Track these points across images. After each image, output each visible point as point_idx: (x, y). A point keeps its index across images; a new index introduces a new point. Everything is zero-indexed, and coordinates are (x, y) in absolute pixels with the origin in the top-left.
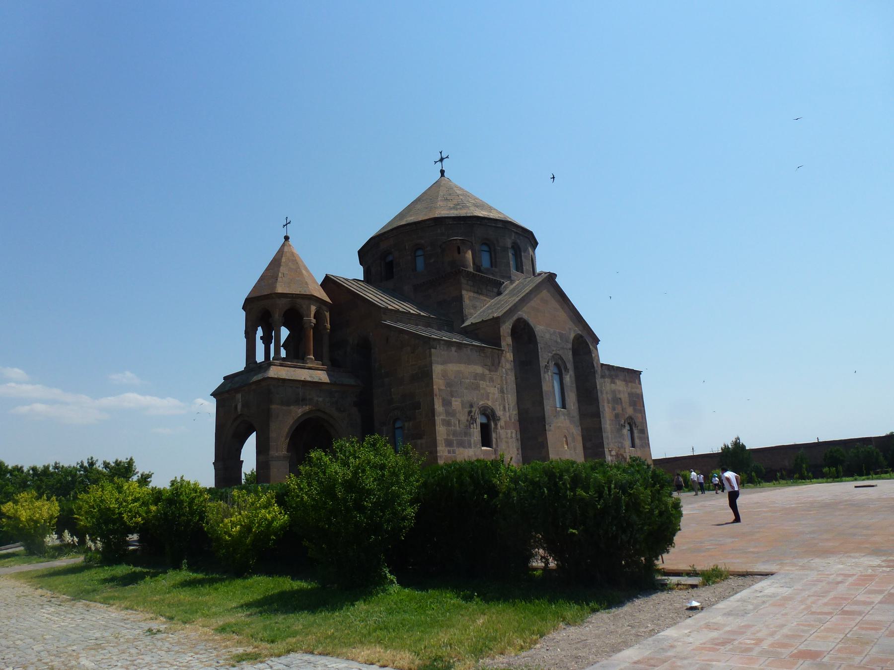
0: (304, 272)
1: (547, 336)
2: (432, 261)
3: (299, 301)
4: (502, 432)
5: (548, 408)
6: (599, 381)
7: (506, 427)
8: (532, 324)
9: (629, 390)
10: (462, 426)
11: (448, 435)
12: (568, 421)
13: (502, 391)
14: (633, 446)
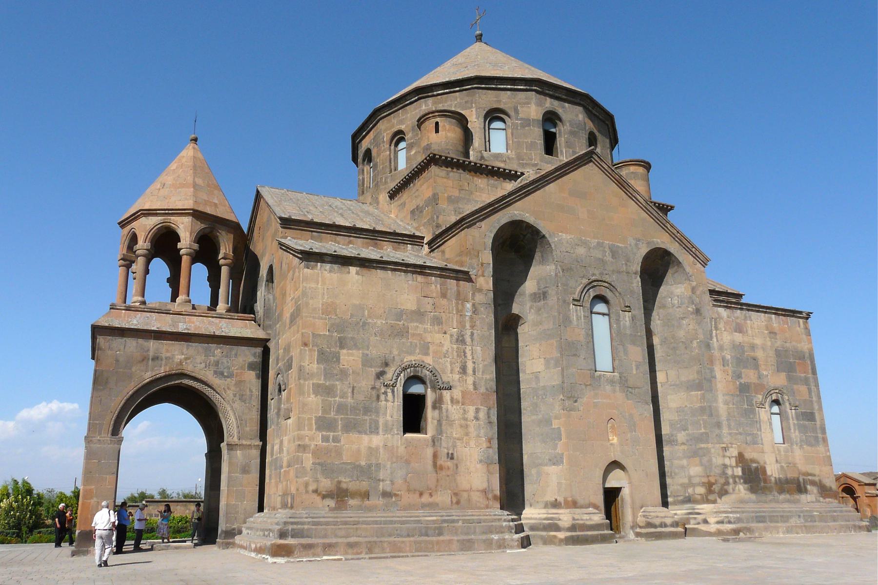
1: (581, 251)
2: (413, 153)
3: (173, 219)
4: (453, 411)
8: (544, 232)
9: (779, 343)
11: (324, 411)
12: (620, 396)
13: (460, 340)
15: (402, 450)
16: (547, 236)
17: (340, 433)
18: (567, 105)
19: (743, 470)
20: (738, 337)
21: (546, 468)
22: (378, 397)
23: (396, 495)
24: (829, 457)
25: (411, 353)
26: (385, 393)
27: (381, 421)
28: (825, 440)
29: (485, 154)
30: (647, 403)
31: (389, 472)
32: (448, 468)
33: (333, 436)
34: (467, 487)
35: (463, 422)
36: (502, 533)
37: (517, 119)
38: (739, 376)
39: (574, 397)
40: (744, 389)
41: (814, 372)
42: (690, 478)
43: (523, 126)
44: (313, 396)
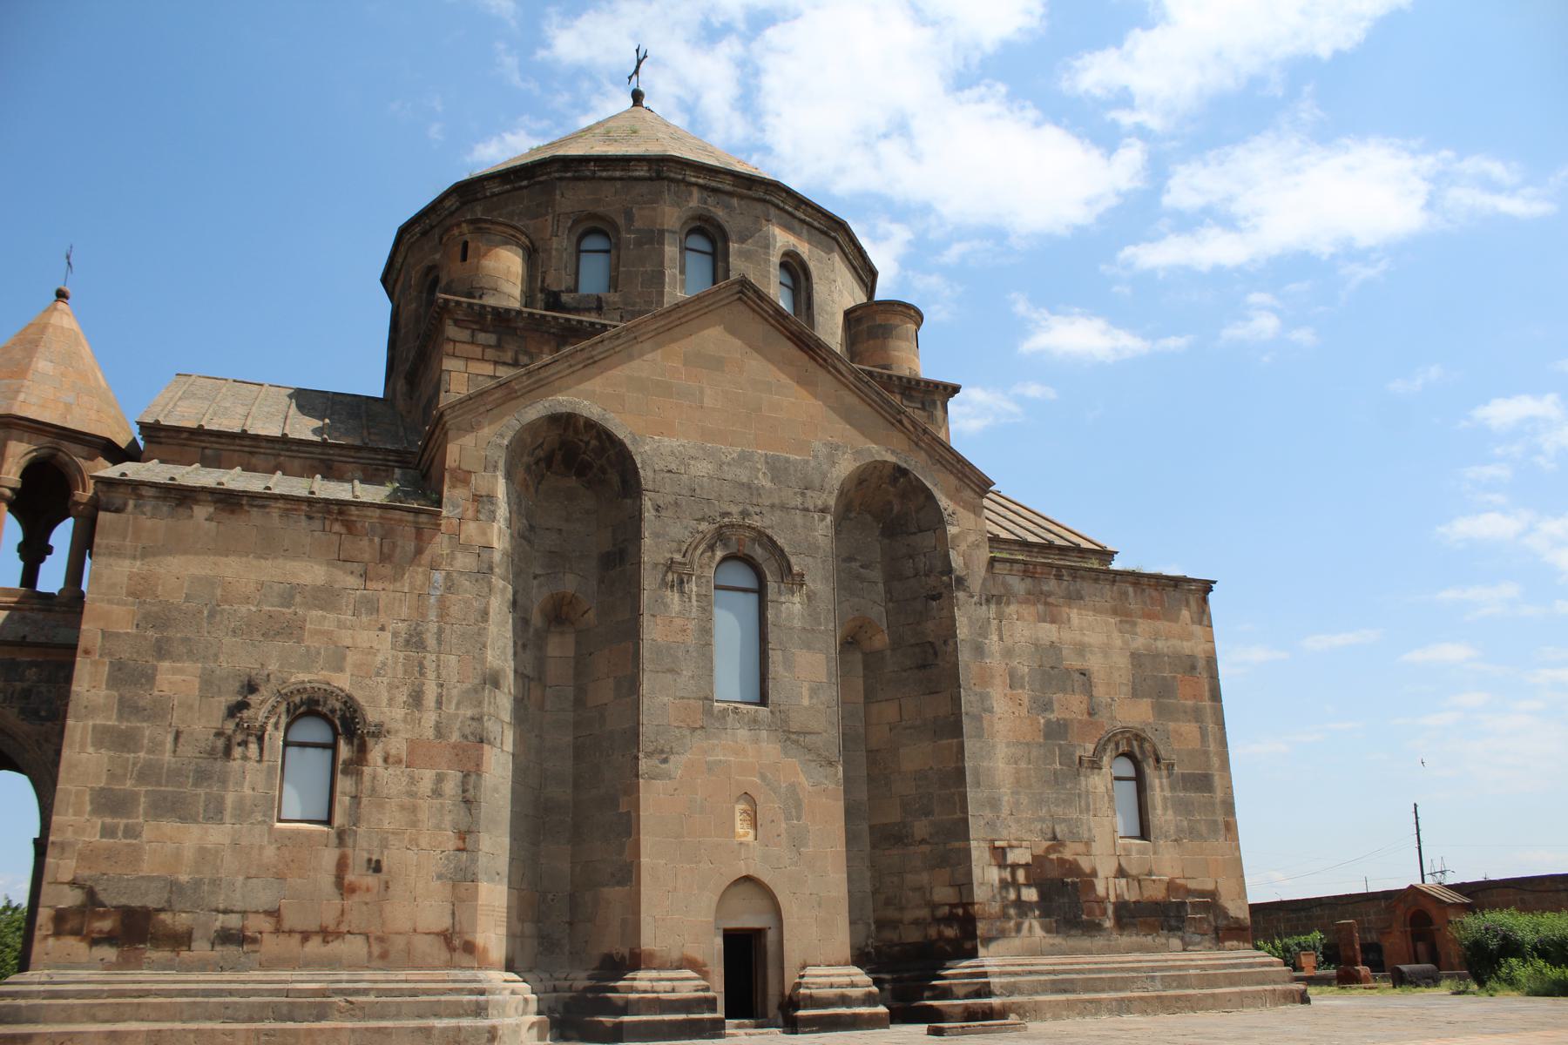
0: (42, 365)
1: (702, 468)
5: (660, 700)
6: (966, 618)
7: (416, 755)
8: (621, 434)
9: (1139, 643)
10: (188, 750)
11: (112, 776)
12: (770, 749)
13: (415, 641)
14: (1144, 834)
15: (270, 852)
16: (628, 442)
17: (141, 820)
18: (735, 201)
19: (1041, 895)
20: (1048, 632)
21: (606, 890)
22: (227, 752)
23: (254, 941)
24: (1237, 863)
25: (307, 669)
26: (244, 743)
27: (230, 798)
28: (1230, 828)
29: (565, 298)
30: (830, 764)
31: (238, 895)
32: (368, 890)
33: (126, 826)
34: (408, 926)
35: (406, 800)
36: (458, 1016)
37: (629, 232)
38: (1047, 706)
39: (662, 751)
40: (1056, 731)
41: (1216, 695)
42: (934, 906)
43: (639, 244)
44: (91, 750)
